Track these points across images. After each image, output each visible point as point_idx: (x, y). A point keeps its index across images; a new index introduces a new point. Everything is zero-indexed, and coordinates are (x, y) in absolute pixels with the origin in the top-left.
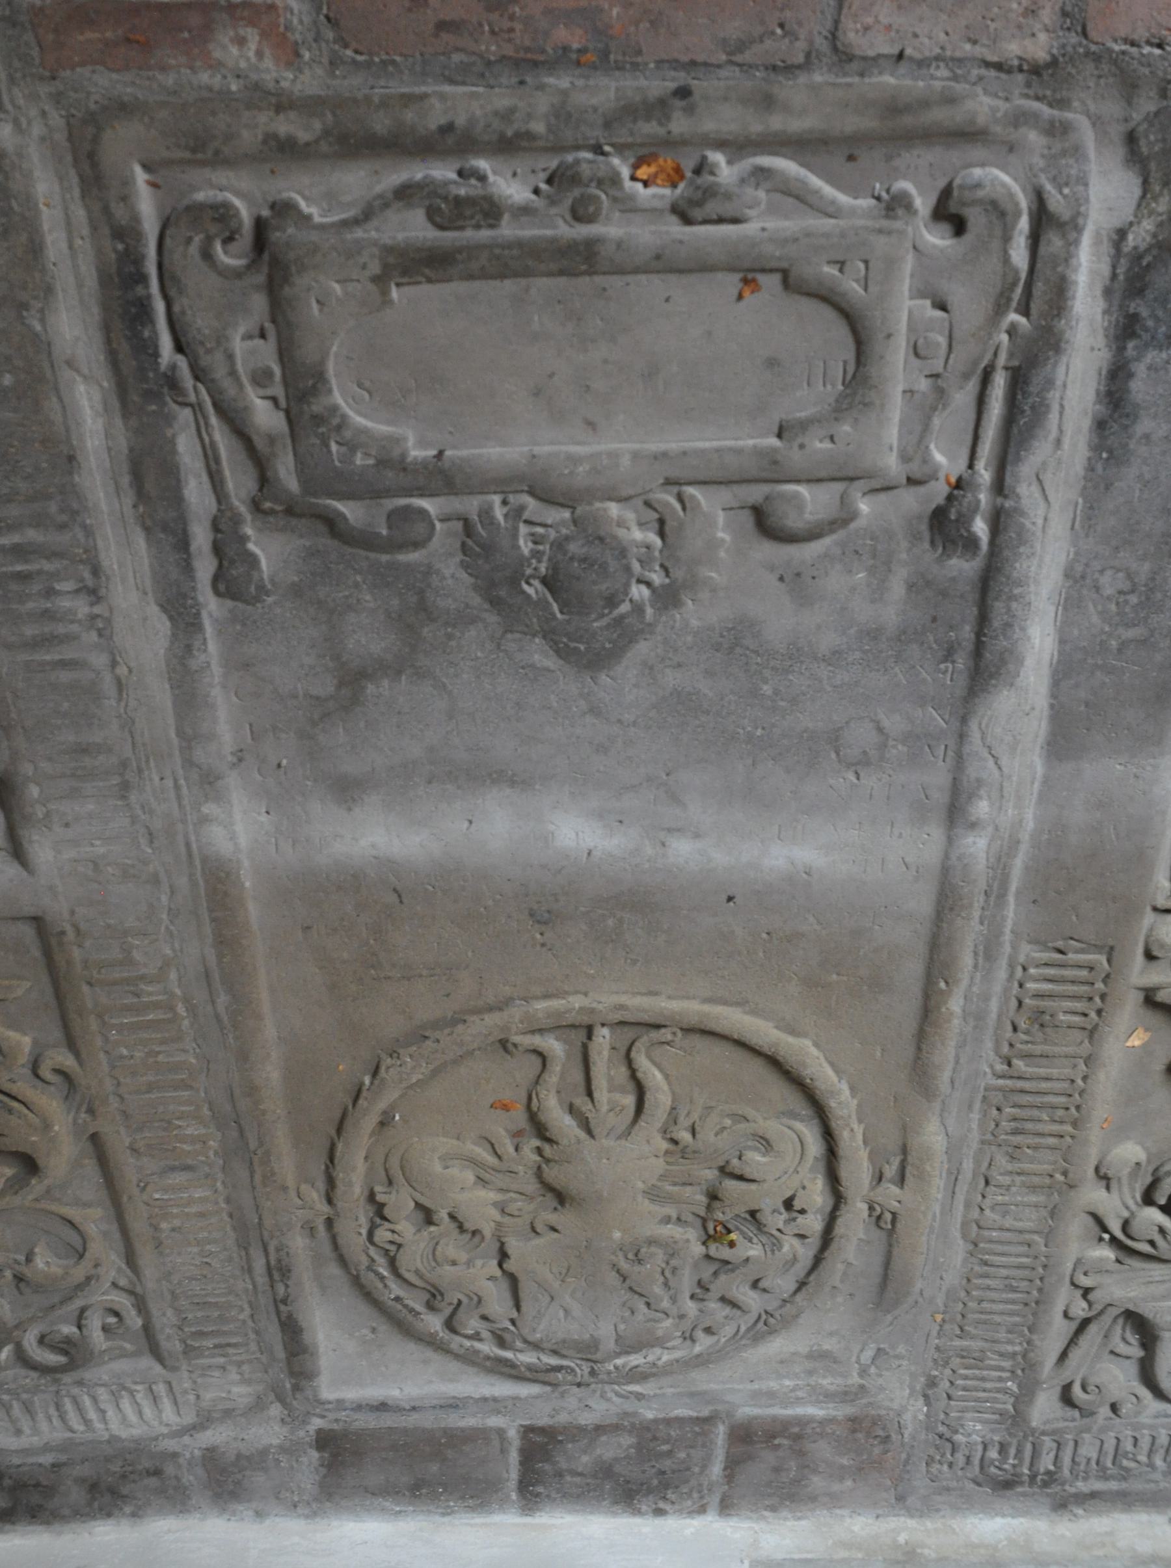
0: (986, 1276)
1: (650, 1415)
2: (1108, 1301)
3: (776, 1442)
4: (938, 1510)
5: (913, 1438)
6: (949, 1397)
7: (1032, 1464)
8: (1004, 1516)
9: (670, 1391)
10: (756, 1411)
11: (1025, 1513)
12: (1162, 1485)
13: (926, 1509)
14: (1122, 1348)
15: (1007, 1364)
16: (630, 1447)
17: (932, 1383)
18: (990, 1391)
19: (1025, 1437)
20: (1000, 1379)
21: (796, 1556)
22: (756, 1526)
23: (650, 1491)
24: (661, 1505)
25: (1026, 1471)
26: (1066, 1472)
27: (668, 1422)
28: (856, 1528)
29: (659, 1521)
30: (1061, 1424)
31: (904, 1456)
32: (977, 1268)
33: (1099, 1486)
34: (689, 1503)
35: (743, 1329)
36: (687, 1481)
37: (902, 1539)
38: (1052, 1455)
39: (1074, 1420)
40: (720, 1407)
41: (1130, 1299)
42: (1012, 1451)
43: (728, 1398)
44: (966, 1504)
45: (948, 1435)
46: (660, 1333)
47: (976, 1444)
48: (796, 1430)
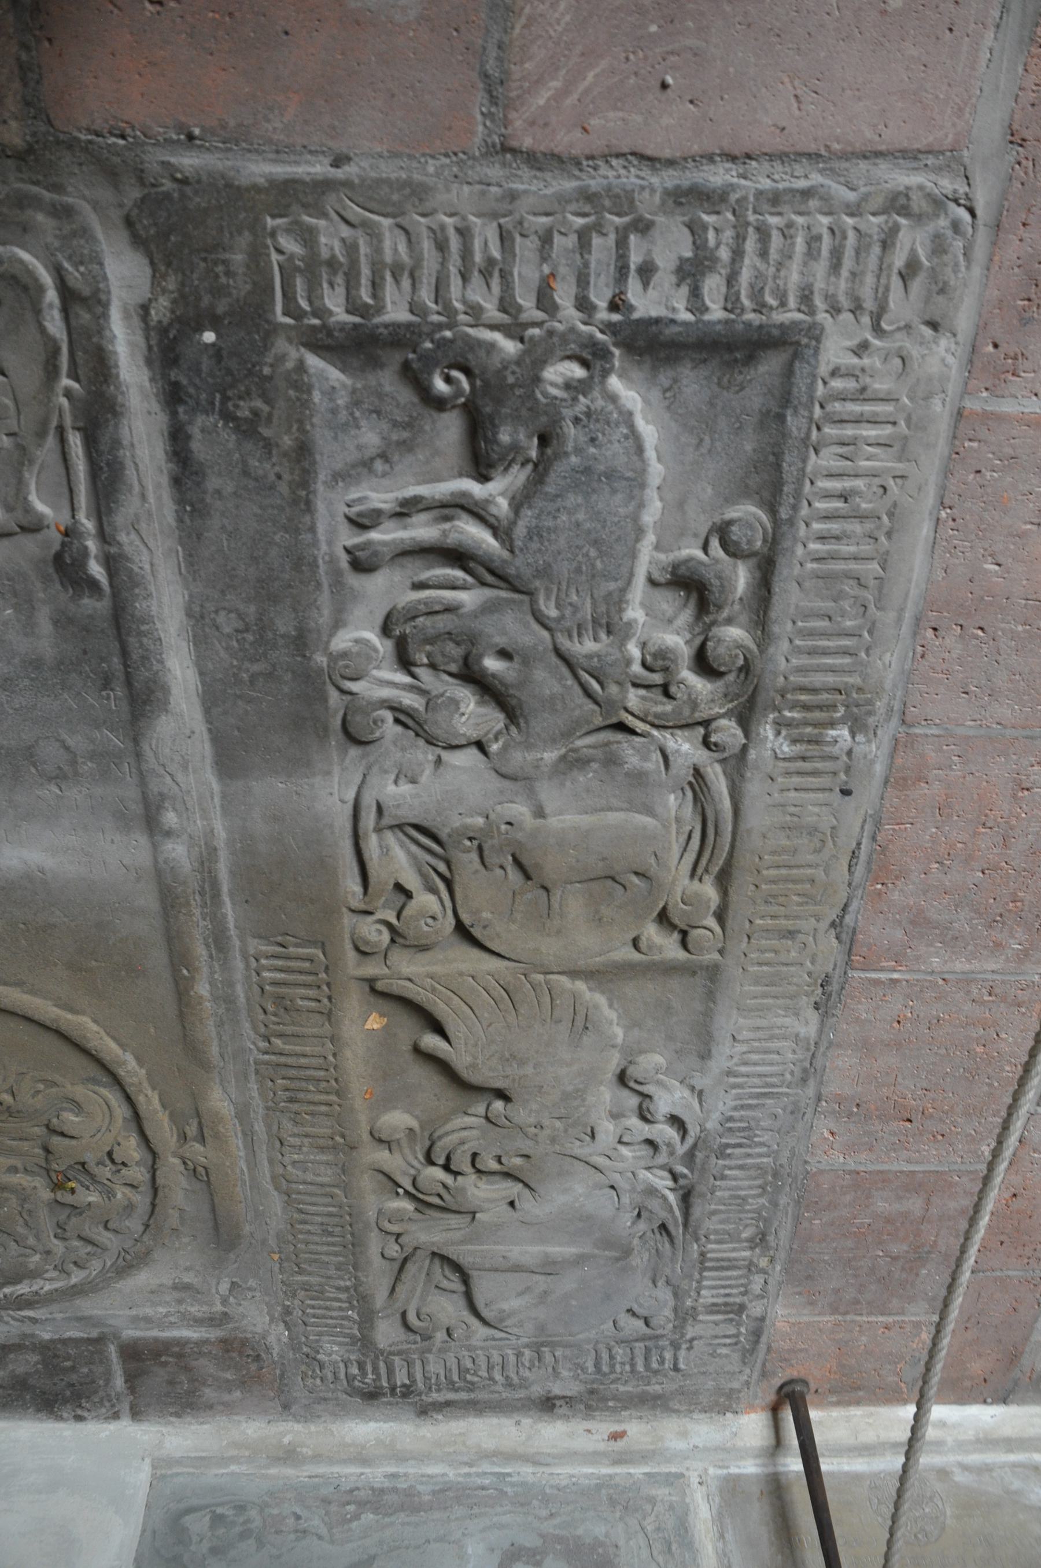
0: (305, 1222)
1: (46, 1336)
2: (415, 1244)
3: (163, 1359)
4: (319, 1417)
5: (282, 1357)
6: (305, 1324)
7: (389, 1380)
8: (376, 1421)
9: (59, 1316)
10: (138, 1334)
11: (395, 1419)
12: (504, 1395)
13: (308, 1416)
14: (445, 1284)
15: (343, 1296)
16: (37, 1363)
17: (287, 1311)
18: (336, 1318)
19: (377, 1357)
20: (341, 1309)
21: (193, 1455)
22: (164, 1430)
23: (65, 1401)
24: (79, 1412)
25: (385, 1384)
26: (420, 1385)
27: (65, 1342)
28: (250, 1432)
29: (80, 1426)
30: (405, 1346)
31: (278, 1372)
32: (296, 1216)
33: (451, 1396)
34: (104, 1410)
35: (109, 1263)
36: (96, 1392)
37: (286, 1440)
38: (405, 1371)
39: (415, 1343)
40: (105, 1330)
41: (433, 1243)
42: (369, 1368)
43: (111, 1322)
44: (341, 1411)
45: (313, 1354)
46: (32, 1267)
47: (336, 1362)
48: (176, 1349)
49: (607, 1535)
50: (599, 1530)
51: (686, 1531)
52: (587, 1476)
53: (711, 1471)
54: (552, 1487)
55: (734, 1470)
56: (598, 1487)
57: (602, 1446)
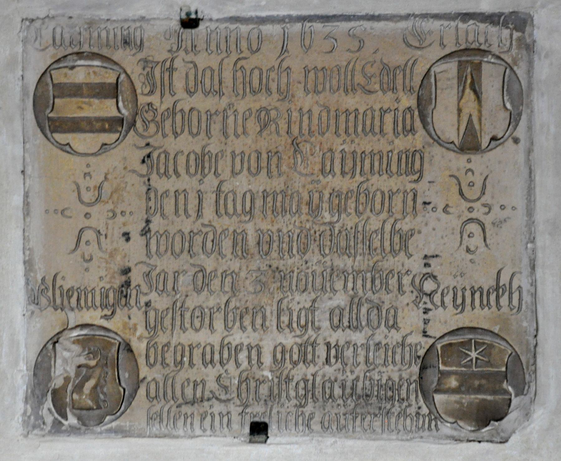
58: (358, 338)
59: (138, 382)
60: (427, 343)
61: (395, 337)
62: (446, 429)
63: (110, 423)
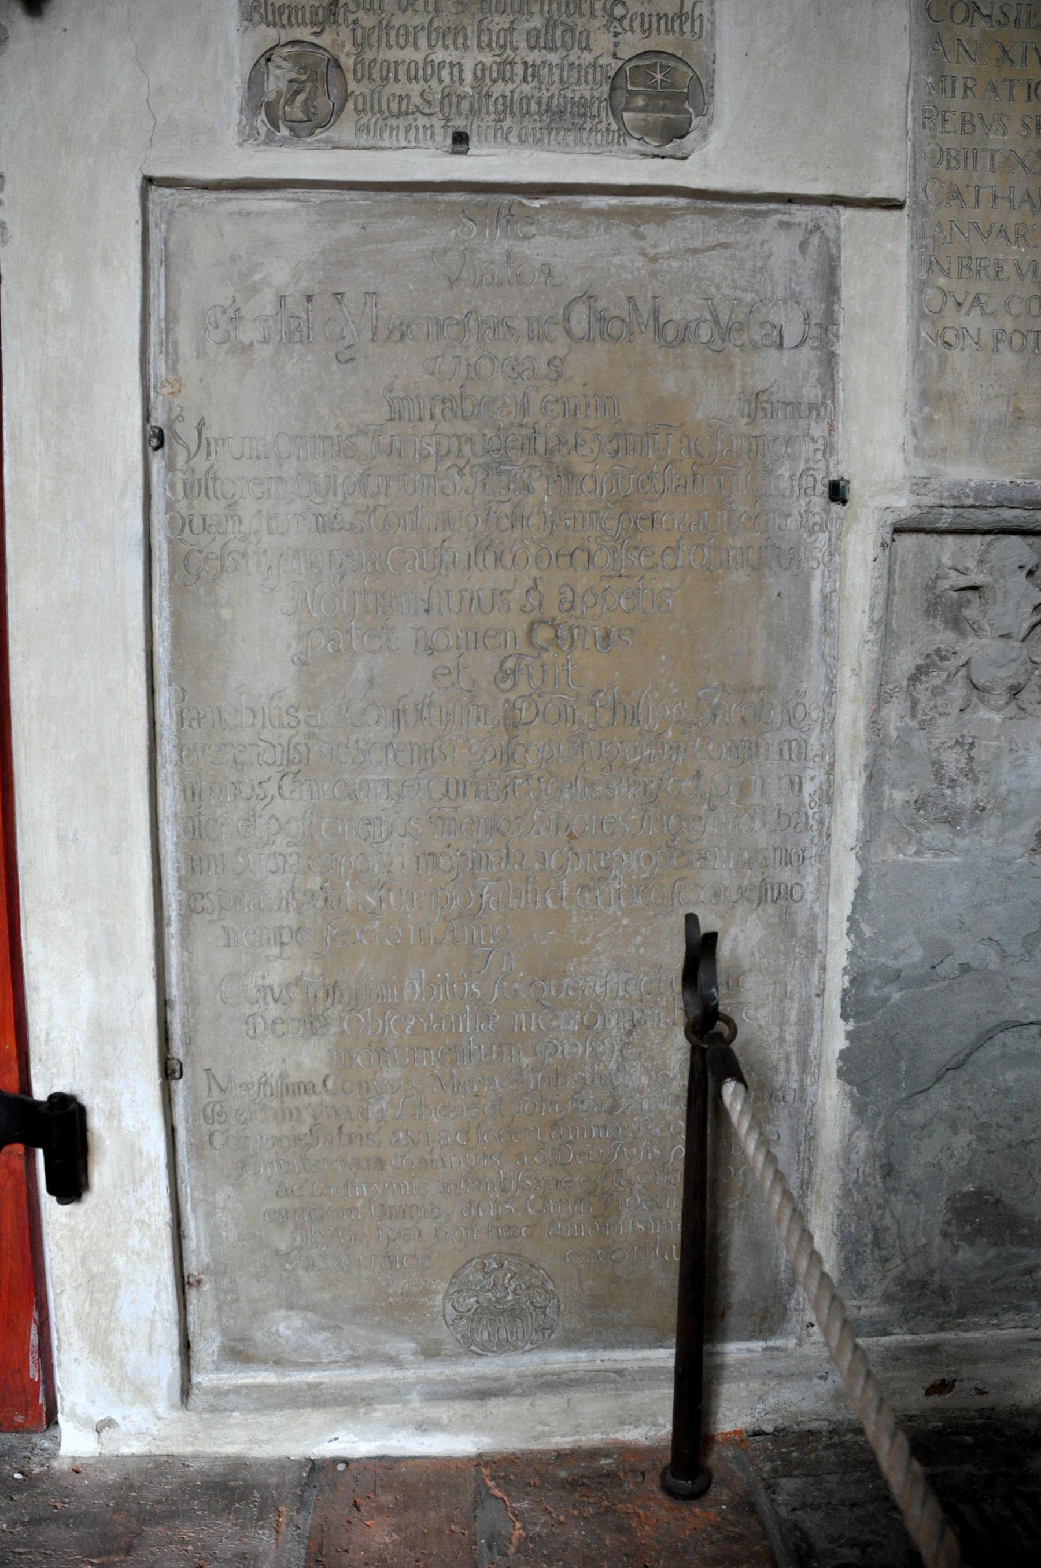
49: (956, 1249)
50: (965, 1255)
51: (846, 1259)
52: (977, 1327)
53: (792, 1342)
54: (1028, 1310)
55: (757, 1345)
56: (961, 1313)
57: (966, 1370)
58: (554, 58)
59: (346, 97)
60: (616, 64)
61: (588, 57)
62: (634, 144)
63: (321, 135)
